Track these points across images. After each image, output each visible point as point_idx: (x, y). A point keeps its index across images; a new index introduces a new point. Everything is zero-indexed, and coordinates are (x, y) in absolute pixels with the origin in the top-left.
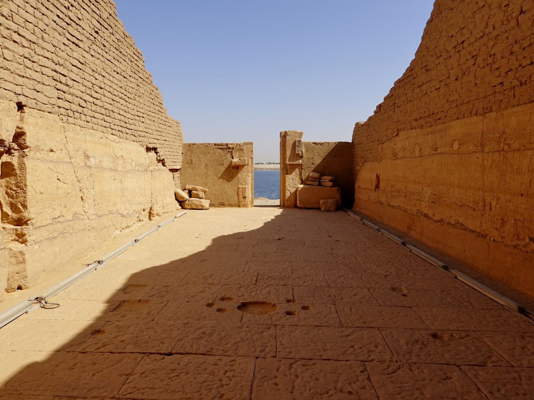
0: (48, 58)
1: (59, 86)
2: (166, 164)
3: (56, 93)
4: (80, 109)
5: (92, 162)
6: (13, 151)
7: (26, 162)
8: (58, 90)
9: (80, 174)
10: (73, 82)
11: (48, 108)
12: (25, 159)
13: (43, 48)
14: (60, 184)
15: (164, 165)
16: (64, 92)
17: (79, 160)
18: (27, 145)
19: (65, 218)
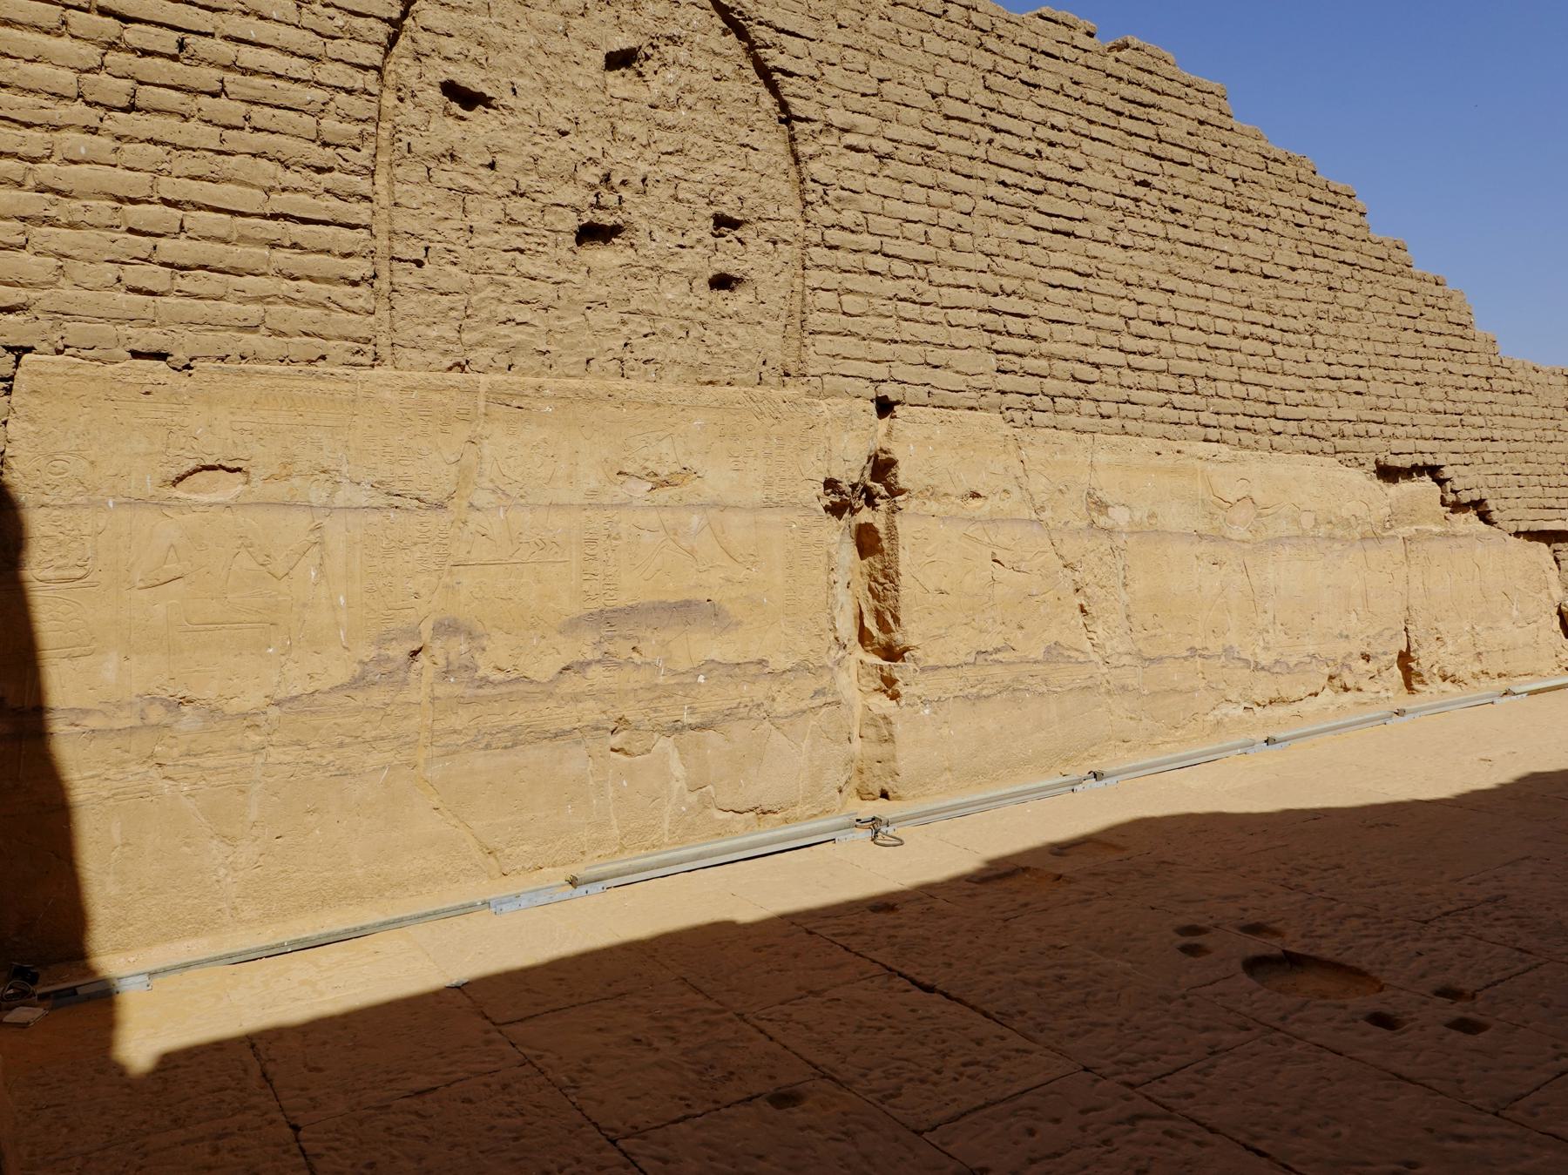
0: (968, 287)
1: (1003, 342)
2: (1495, 516)
4: (1076, 389)
5: (1119, 516)
6: (877, 500)
7: (897, 524)
8: (998, 352)
9: (1070, 548)
10: (1054, 326)
11: (971, 398)
12: (897, 518)
13: (953, 268)
14: (1001, 573)
15: (1485, 517)
16: (1021, 355)
17: (1073, 512)
18: (901, 485)
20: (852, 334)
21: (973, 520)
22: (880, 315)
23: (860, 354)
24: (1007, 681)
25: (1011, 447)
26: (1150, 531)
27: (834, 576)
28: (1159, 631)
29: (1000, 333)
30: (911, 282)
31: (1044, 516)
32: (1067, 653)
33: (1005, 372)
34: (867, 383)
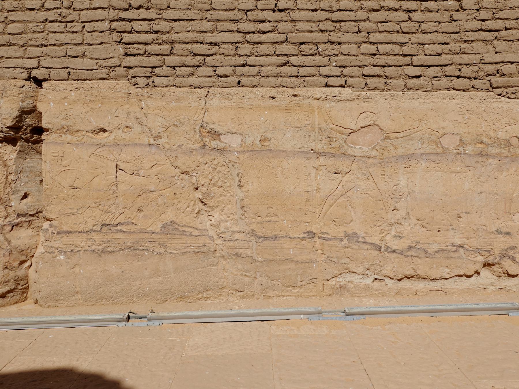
0: (103, 8)
1: (127, 38)
3: (121, 49)
9: (185, 162)
16: (146, 44)
19: (138, 227)
20: (15, 45)
21: (100, 145)
22: (34, 32)
23: (18, 55)
24: (128, 244)
25: (134, 100)
26: (263, 149)
27: (12, 177)
28: (273, 218)
29: (130, 32)
30: (59, 11)
31: (159, 141)
32: (181, 229)
33: (134, 55)
34: (21, 70)
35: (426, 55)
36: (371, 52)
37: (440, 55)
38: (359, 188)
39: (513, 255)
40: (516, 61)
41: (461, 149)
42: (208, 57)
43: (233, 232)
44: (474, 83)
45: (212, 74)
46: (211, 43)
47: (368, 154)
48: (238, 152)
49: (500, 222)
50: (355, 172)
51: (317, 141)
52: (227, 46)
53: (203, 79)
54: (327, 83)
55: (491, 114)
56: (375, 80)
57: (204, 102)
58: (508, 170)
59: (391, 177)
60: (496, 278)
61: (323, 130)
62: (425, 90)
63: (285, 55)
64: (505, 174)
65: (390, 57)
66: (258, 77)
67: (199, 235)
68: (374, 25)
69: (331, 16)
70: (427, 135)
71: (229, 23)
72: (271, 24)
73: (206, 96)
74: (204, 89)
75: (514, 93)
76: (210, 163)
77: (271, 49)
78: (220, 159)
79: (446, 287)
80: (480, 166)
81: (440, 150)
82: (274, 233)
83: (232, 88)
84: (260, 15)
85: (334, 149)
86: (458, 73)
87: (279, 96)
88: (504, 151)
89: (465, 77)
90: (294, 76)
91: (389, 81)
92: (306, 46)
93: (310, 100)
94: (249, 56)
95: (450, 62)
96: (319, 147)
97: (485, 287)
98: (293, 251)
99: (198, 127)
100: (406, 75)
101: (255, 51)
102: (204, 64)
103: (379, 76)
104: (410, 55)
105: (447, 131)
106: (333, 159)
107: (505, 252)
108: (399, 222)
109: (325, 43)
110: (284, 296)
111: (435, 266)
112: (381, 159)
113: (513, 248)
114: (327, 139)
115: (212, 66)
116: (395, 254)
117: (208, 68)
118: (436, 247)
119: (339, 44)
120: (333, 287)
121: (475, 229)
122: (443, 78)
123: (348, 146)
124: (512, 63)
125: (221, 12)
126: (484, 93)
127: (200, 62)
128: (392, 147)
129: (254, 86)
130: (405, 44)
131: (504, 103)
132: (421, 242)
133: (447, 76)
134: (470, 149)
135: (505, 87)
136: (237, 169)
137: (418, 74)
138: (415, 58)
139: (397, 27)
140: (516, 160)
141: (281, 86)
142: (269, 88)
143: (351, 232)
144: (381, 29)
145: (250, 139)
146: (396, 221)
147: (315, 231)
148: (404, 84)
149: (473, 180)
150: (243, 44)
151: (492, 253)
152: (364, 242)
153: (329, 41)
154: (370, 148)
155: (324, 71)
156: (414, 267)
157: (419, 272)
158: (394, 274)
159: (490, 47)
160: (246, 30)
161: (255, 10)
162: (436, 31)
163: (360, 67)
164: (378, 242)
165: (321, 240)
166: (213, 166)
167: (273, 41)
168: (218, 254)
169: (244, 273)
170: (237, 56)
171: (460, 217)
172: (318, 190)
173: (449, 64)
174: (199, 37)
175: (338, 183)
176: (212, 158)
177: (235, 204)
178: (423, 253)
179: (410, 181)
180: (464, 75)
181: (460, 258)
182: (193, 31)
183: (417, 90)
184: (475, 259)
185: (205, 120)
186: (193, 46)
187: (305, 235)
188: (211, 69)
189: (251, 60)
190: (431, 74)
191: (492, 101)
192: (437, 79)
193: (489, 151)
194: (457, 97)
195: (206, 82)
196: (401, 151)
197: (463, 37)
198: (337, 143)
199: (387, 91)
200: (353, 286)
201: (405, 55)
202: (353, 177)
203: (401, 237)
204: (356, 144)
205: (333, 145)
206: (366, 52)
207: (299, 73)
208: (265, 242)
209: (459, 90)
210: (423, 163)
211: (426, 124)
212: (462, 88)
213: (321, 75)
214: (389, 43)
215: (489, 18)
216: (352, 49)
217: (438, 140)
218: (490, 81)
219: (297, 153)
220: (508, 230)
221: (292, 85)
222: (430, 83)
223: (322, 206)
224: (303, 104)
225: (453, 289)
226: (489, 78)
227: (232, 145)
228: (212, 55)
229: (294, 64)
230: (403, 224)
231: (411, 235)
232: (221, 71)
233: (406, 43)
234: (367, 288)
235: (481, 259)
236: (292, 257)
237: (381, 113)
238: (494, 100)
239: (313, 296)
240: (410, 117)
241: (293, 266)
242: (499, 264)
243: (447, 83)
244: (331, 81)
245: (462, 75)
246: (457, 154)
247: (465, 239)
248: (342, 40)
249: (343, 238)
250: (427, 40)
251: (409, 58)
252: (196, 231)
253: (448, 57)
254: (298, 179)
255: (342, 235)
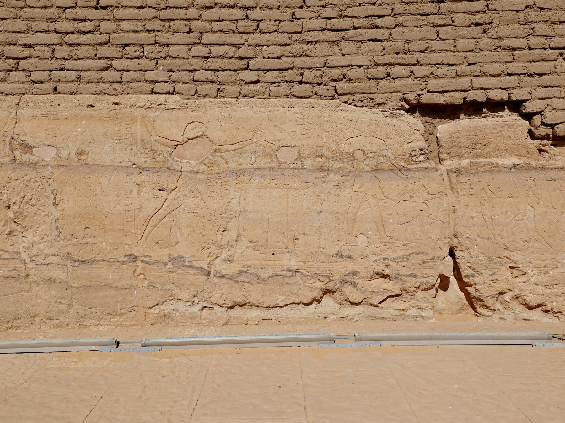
26: (79, 164)
28: (91, 240)
35: (264, 58)
36: (202, 55)
37: (279, 58)
38: (185, 207)
39: (356, 281)
40: (364, 64)
41: (299, 163)
42: (22, 61)
43: (47, 255)
44: (317, 89)
45: (25, 79)
46: (24, 45)
47: (196, 169)
48: (52, 167)
49: (341, 244)
50: (182, 189)
51: (139, 154)
52: (42, 48)
53: (16, 85)
54: (153, 89)
55: (334, 124)
56: (207, 86)
57: (15, 111)
58: (352, 187)
59: (221, 195)
60: (337, 305)
61: (146, 142)
62: (261, 97)
63: (108, 58)
64: (348, 191)
65: (224, 60)
66: (77, 83)
67: (9, 259)
68: (207, 25)
69: (158, 13)
70: (261, 147)
71: (45, 22)
72: (92, 23)
73: (18, 105)
74: (16, 96)
75: (362, 101)
76: (22, 179)
77: (91, 52)
78: (32, 174)
79: (279, 316)
80: (320, 182)
81: (275, 165)
82: (92, 256)
83: (47, 96)
84: (80, 13)
85: (158, 163)
86: (299, 78)
87: (98, 105)
88: (346, 165)
89: (307, 83)
90: (116, 82)
91: (222, 87)
92: (131, 48)
93: (133, 109)
94: (67, 59)
95: (291, 66)
96: (141, 161)
97: (325, 315)
98: (112, 275)
99: (8, 139)
100: (242, 80)
101: (74, 54)
102: (17, 68)
103: (212, 82)
104: (247, 58)
105: (284, 143)
106: (157, 174)
107: (346, 278)
108: (230, 244)
109: (152, 44)
110: (102, 325)
111: (268, 292)
112: (210, 174)
113: (355, 273)
114: (152, 153)
115: (26, 71)
116: (224, 279)
117: (21, 73)
118: (270, 272)
119: (168, 45)
120: (156, 315)
121: (313, 252)
122: (283, 84)
123: (173, 160)
124: (360, 67)
125: (37, 10)
126: (328, 100)
127: (13, 65)
128: (223, 161)
129: (72, 94)
130: (241, 46)
131: (349, 111)
132: (253, 266)
133: (287, 82)
134: (308, 163)
135: (353, 94)
136: (51, 186)
137: (255, 79)
138: (252, 61)
139: (233, 27)
140: (360, 176)
141: (101, 93)
142: (88, 96)
143: (176, 255)
144: (215, 29)
145: (66, 152)
146: (227, 243)
147: (136, 254)
148: (238, 90)
149: (312, 198)
150: (61, 45)
151: (331, 278)
152: (190, 267)
153: (156, 43)
154: (198, 162)
155: (150, 76)
156: (245, 293)
157: (250, 300)
158: (223, 302)
159: (337, 48)
160: (63, 30)
161: (74, 7)
162: (276, 31)
163: (190, 71)
164: (206, 267)
165: (144, 264)
166: (25, 182)
167: (94, 42)
168: (30, 279)
169: (59, 300)
170: (55, 59)
171: (297, 239)
172: (140, 208)
173: (289, 68)
174: (11, 39)
175: (163, 201)
176: (23, 173)
177: (49, 224)
178: (256, 279)
179: (242, 199)
180: (306, 81)
181: (296, 283)
182: (6, 31)
183: (253, 97)
184: (313, 285)
185: (16, 131)
186: (5, 48)
187: (126, 259)
188: (25, 74)
189: (69, 64)
190: (269, 79)
191: (336, 110)
192: (276, 84)
193: (330, 165)
194: (297, 105)
195: (18, 89)
196: (232, 165)
197: (305, 37)
198: (161, 157)
199: (220, 99)
200: (178, 314)
201: (241, 58)
202: (179, 194)
203: (231, 261)
204: (182, 158)
205: (157, 158)
206: (197, 55)
207: (122, 78)
208: (81, 266)
209: (301, 97)
210: (257, 179)
211: (261, 136)
212: (303, 95)
213: (146, 81)
214: (224, 45)
215: (336, 16)
216: (182, 51)
217: (273, 154)
218: (335, 87)
219: (116, 168)
220: (350, 254)
221: (114, 92)
222: (268, 89)
223: (145, 227)
224: (124, 114)
225: (288, 318)
226: (334, 84)
227: (45, 159)
228: (25, 58)
229: (116, 68)
230: (234, 246)
231: (242, 259)
232: (35, 76)
233: (241, 44)
234: (192, 317)
235: (319, 285)
236: (111, 282)
237: (210, 123)
238: (339, 108)
239: (133, 325)
240: (244, 128)
241: (112, 292)
242: (340, 290)
243: (285, 90)
244: (158, 87)
245: (304, 80)
246: (295, 168)
247: (302, 264)
248: (171, 41)
249: (167, 261)
250: (265, 40)
251: (245, 61)
252: (6, 254)
253: (289, 59)
254: (119, 196)
255: (166, 259)
